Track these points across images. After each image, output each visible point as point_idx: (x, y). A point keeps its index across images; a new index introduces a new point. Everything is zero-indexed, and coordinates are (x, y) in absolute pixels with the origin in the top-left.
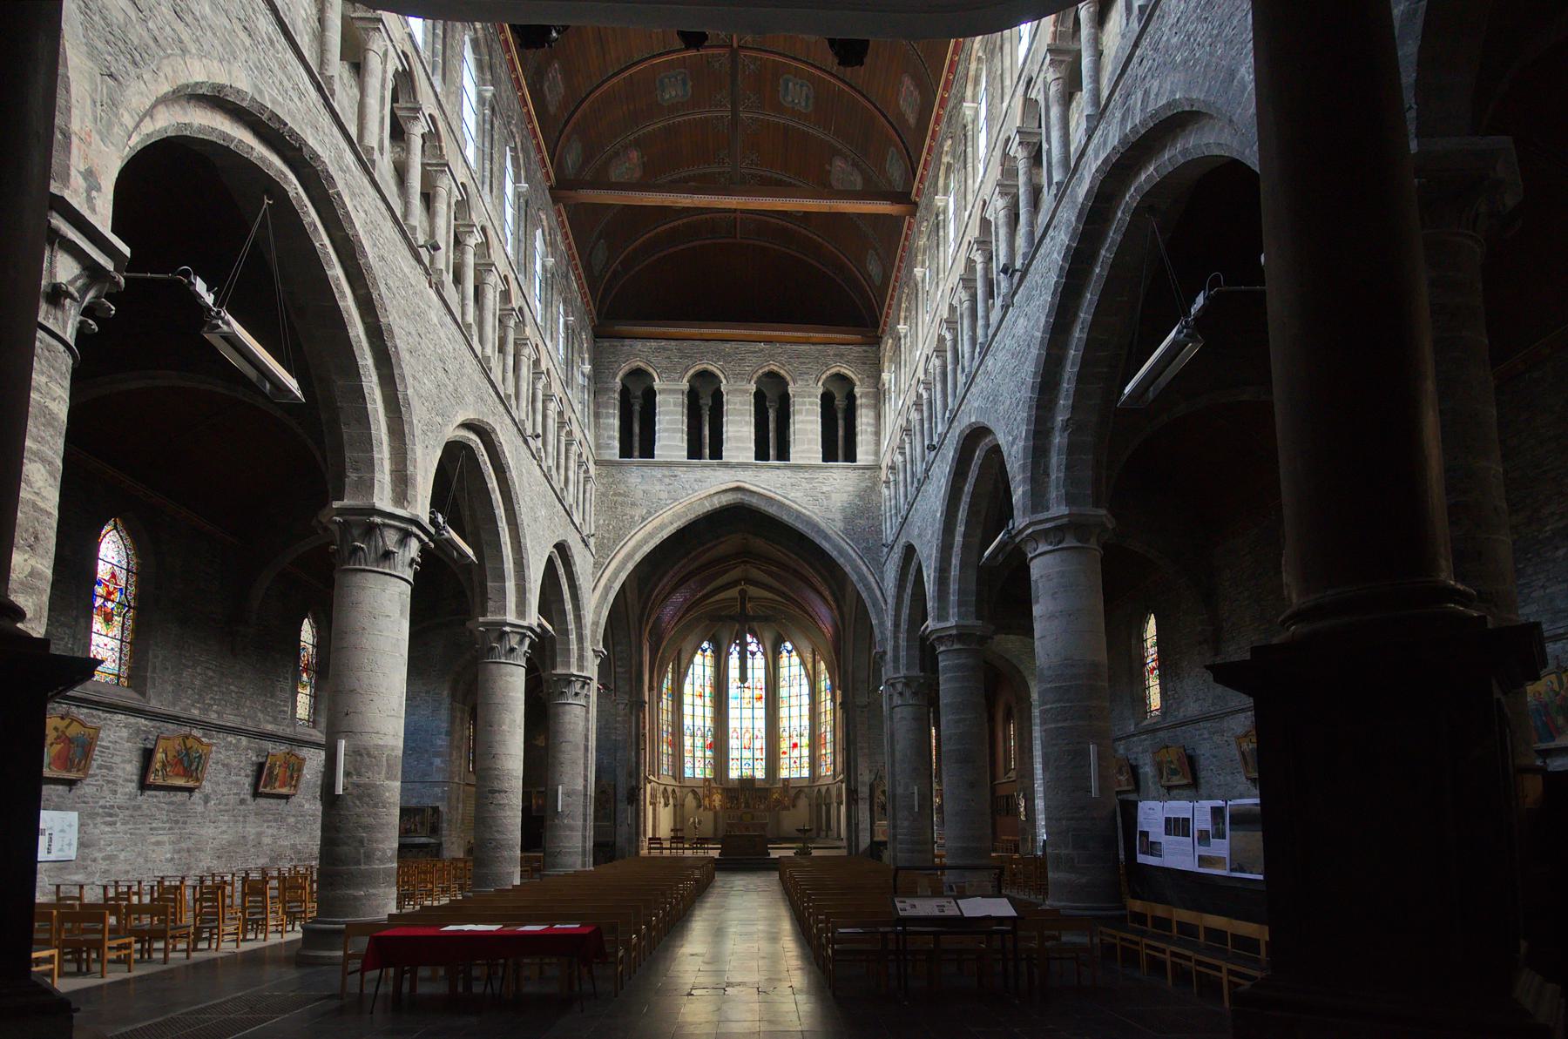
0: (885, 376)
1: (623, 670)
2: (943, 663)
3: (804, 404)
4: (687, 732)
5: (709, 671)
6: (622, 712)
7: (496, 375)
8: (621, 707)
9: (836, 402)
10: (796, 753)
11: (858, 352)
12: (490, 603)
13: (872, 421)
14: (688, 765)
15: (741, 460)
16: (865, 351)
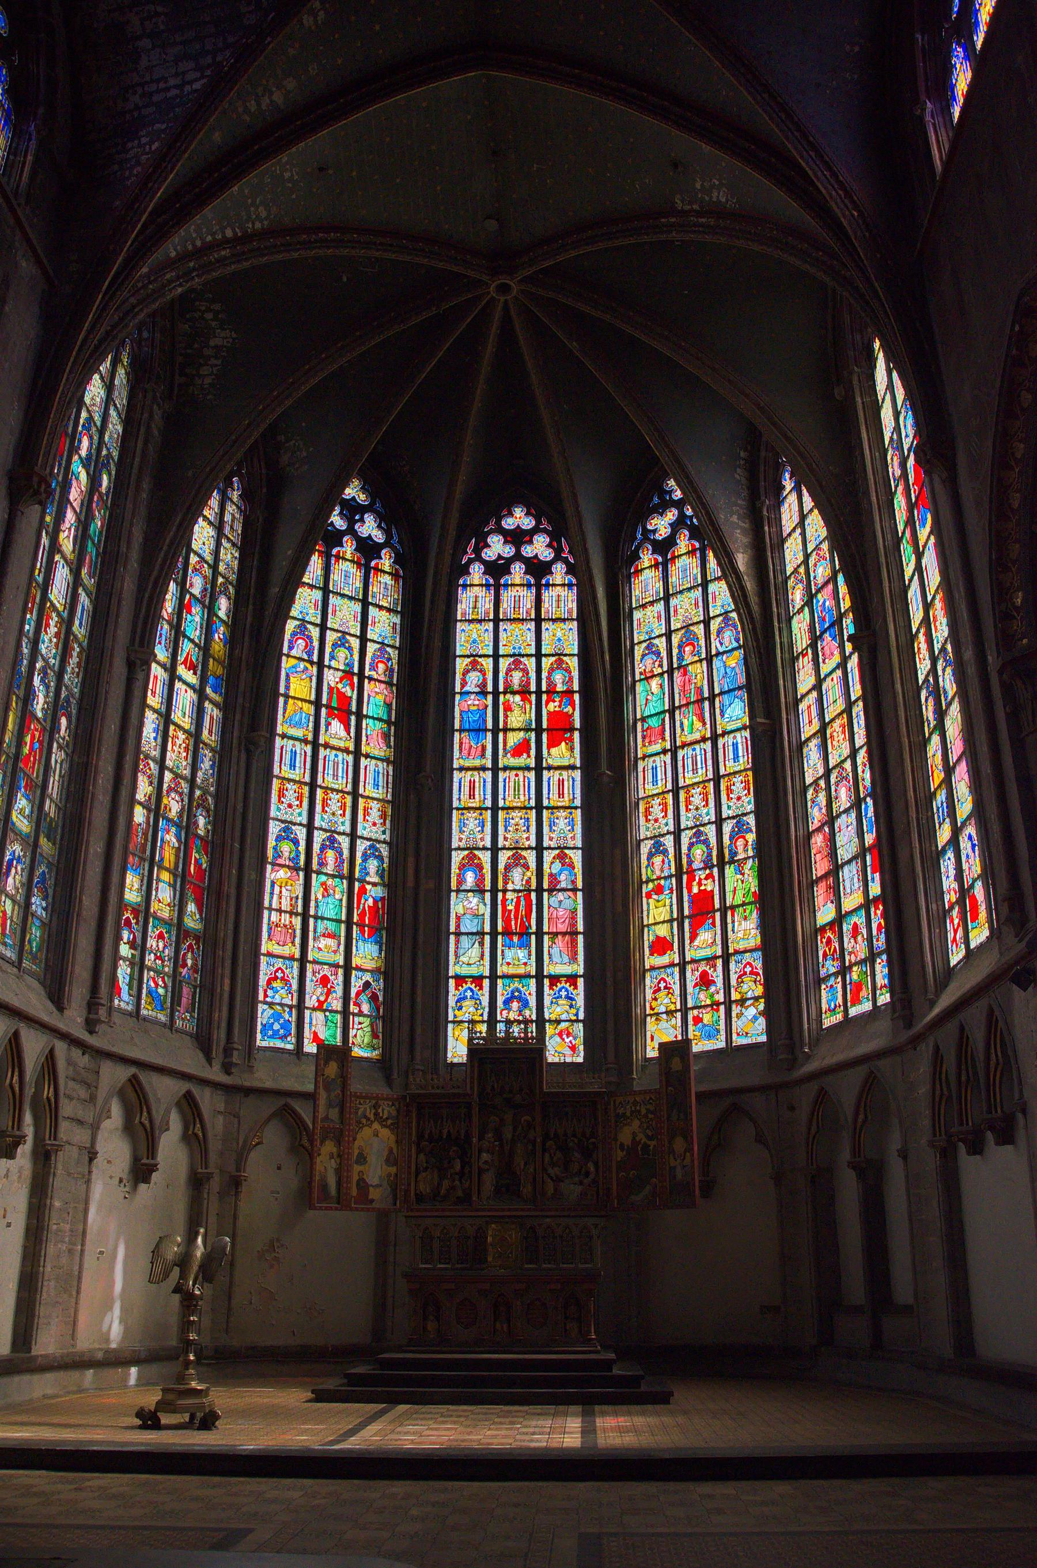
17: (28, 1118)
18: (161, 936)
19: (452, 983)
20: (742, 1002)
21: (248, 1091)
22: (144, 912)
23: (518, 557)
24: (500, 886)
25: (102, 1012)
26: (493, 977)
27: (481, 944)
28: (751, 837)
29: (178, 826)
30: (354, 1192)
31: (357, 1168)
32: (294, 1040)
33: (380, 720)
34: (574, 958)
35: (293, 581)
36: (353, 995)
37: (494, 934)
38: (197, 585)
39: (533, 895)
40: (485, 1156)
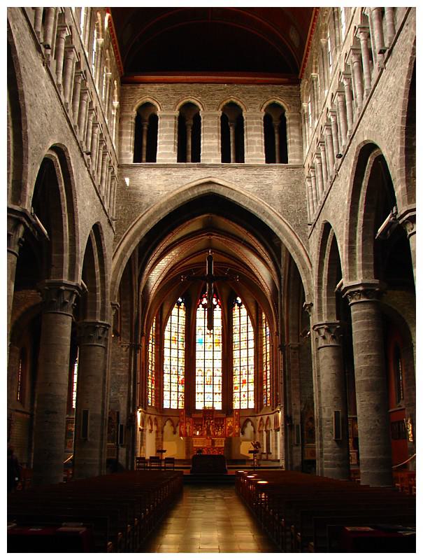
0: (304, 105)
1: (126, 320)
2: (355, 312)
3: (253, 123)
4: (166, 371)
5: (182, 321)
6: (124, 353)
7: (70, 115)
8: (124, 349)
9: (274, 122)
10: (244, 389)
11: (287, 89)
12: (53, 269)
13: (297, 135)
14: (166, 395)
15: (212, 162)
16: (291, 89)
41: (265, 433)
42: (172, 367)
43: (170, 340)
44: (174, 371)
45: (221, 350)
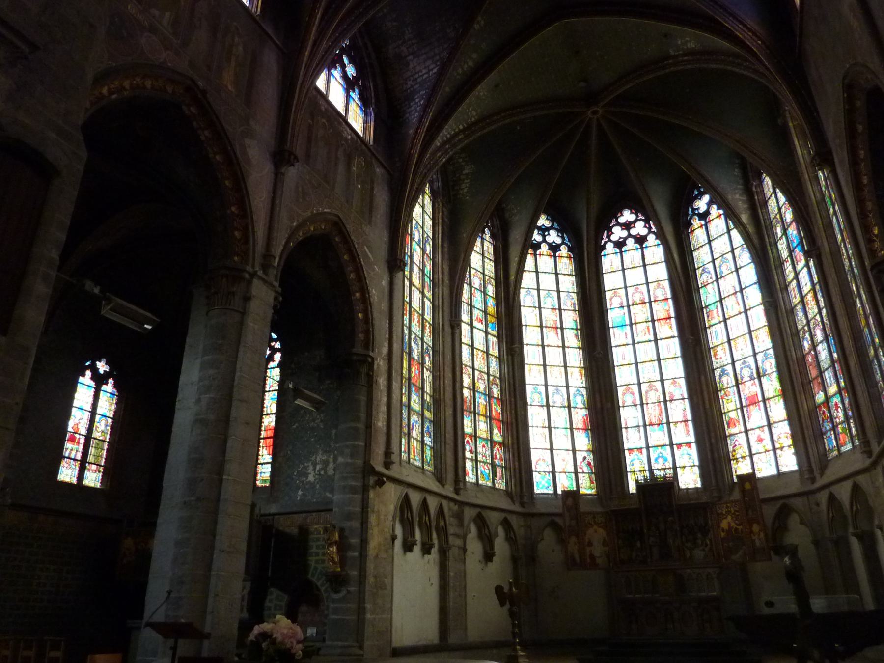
17: (434, 535)
18: (484, 446)
19: (627, 452)
20: (782, 448)
21: (533, 515)
22: (475, 436)
23: (630, 236)
24: (645, 402)
25: (461, 485)
26: (648, 448)
27: (639, 431)
28: (773, 361)
29: (485, 394)
30: (589, 560)
31: (588, 549)
32: (552, 488)
33: (572, 329)
34: (688, 434)
35: (520, 269)
36: (578, 463)
37: (645, 426)
38: (476, 282)
39: (662, 404)
40: (652, 539)
41: (856, 545)
42: (550, 389)
43: (541, 327)
44: (558, 399)
45: (675, 332)
